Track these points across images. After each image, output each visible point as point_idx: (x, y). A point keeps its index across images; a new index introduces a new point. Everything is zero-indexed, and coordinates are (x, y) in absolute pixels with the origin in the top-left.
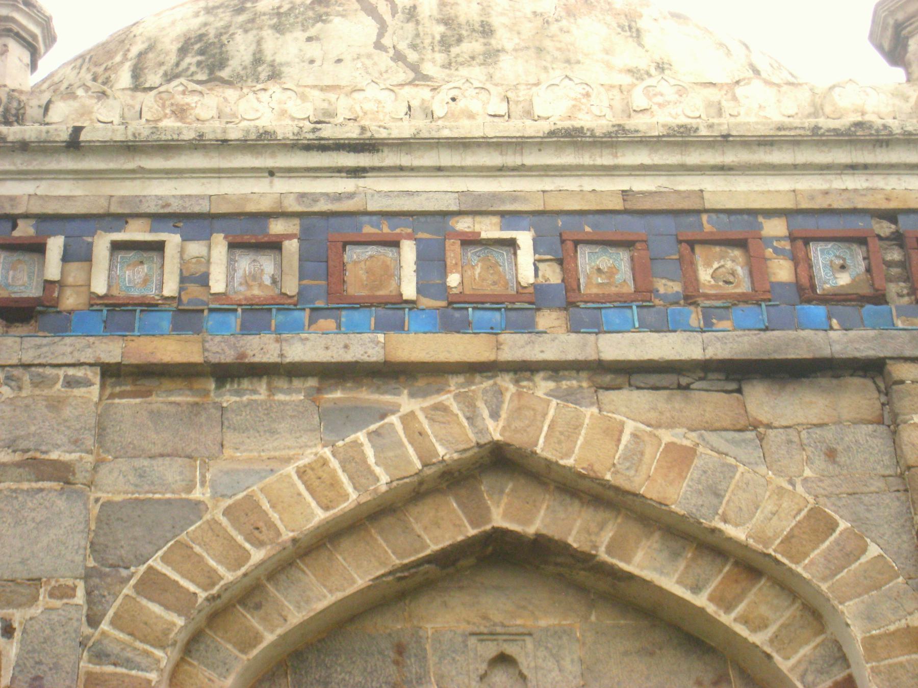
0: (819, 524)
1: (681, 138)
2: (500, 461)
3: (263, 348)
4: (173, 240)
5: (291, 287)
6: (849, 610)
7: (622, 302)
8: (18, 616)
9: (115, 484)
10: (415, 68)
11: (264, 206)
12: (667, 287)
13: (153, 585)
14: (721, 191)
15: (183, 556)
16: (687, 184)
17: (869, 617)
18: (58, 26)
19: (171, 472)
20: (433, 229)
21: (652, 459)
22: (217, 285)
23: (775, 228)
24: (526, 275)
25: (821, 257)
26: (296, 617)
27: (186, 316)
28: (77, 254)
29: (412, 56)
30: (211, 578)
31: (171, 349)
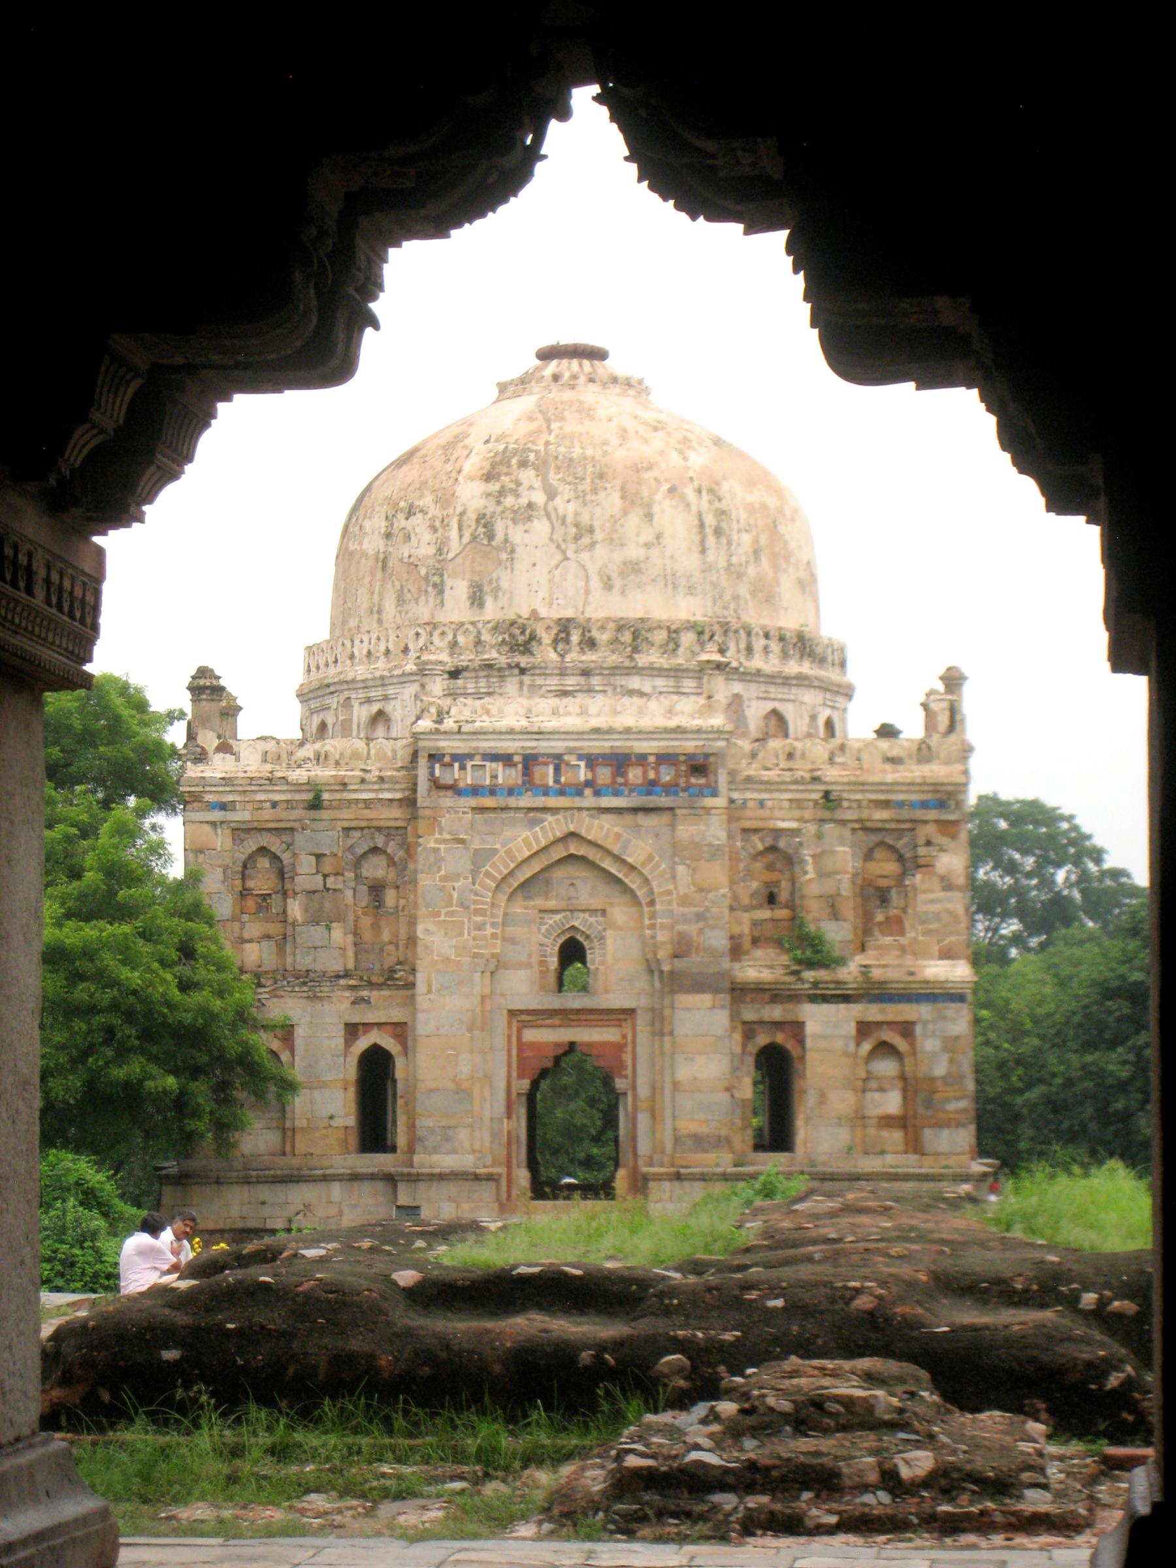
0: (650, 858)
1: (628, 731)
2: (572, 835)
3: (512, 802)
4: (488, 764)
5: (520, 782)
6: (654, 884)
7: (607, 786)
8: (456, 885)
9: (476, 845)
10: (564, 552)
11: (511, 751)
12: (620, 780)
13: (487, 874)
15: (494, 866)
16: (629, 744)
17: (659, 886)
19: (489, 838)
20: (558, 761)
21: (612, 836)
22: (500, 781)
23: (652, 759)
24: (582, 778)
25: (663, 769)
26: (522, 879)
27: (493, 792)
28: (463, 768)
29: (563, 546)
30: (500, 872)
31: (489, 802)
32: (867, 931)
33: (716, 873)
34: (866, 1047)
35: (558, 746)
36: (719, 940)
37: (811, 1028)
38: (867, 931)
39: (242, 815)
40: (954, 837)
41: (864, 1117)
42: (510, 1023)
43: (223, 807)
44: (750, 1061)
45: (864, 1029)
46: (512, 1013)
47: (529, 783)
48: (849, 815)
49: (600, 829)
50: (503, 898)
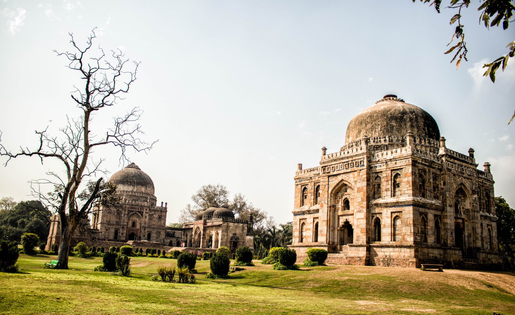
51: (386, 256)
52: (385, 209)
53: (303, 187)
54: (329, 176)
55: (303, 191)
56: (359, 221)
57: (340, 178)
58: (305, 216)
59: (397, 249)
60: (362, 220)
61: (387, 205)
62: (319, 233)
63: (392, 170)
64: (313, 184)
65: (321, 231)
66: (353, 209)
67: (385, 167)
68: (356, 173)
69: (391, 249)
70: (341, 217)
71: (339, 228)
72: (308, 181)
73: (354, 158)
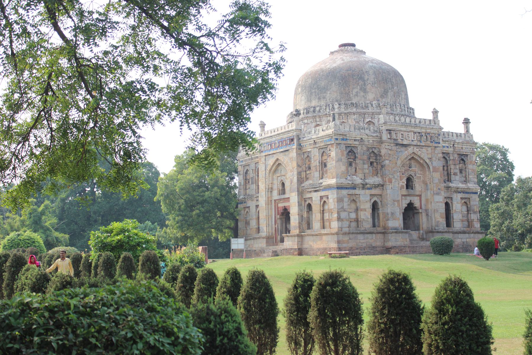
2: (278, 159)
14: (285, 136)
18: (265, 123)
32: (323, 174)
33: (295, 164)
34: (322, 202)
35: (274, 139)
36: (295, 180)
37: (313, 199)
38: (323, 174)
39: (244, 163)
40: (332, 147)
41: (323, 220)
42: (275, 203)
43: (242, 161)
44: (306, 207)
45: (321, 198)
46: (275, 200)
47: (271, 148)
48: (317, 146)
49: (281, 157)
50: (271, 174)
51: (464, 242)
52: (455, 194)
53: (349, 149)
54: (397, 144)
55: (348, 154)
56: (437, 204)
57: (410, 150)
58: (357, 192)
59: (472, 235)
60: (441, 204)
61: (457, 191)
62: (390, 216)
63: (458, 154)
64: (365, 148)
65: (392, 214)
66: (420, 190)
67: (452, 149)
68: (429, 149)
69: (467, 235)
70: (403, 197)
71: (403, 211)
72: (357, 143)
73: (428, 131)
